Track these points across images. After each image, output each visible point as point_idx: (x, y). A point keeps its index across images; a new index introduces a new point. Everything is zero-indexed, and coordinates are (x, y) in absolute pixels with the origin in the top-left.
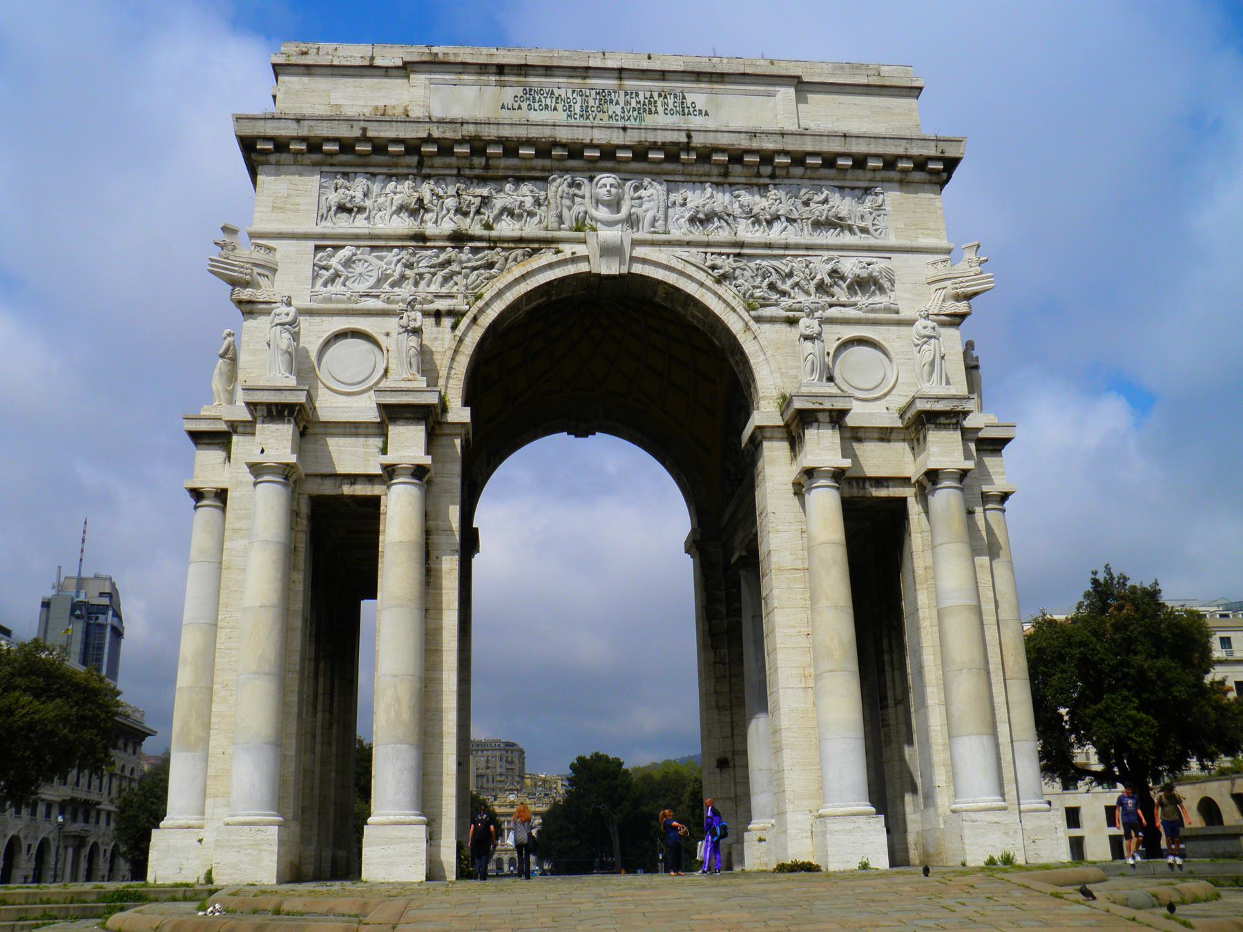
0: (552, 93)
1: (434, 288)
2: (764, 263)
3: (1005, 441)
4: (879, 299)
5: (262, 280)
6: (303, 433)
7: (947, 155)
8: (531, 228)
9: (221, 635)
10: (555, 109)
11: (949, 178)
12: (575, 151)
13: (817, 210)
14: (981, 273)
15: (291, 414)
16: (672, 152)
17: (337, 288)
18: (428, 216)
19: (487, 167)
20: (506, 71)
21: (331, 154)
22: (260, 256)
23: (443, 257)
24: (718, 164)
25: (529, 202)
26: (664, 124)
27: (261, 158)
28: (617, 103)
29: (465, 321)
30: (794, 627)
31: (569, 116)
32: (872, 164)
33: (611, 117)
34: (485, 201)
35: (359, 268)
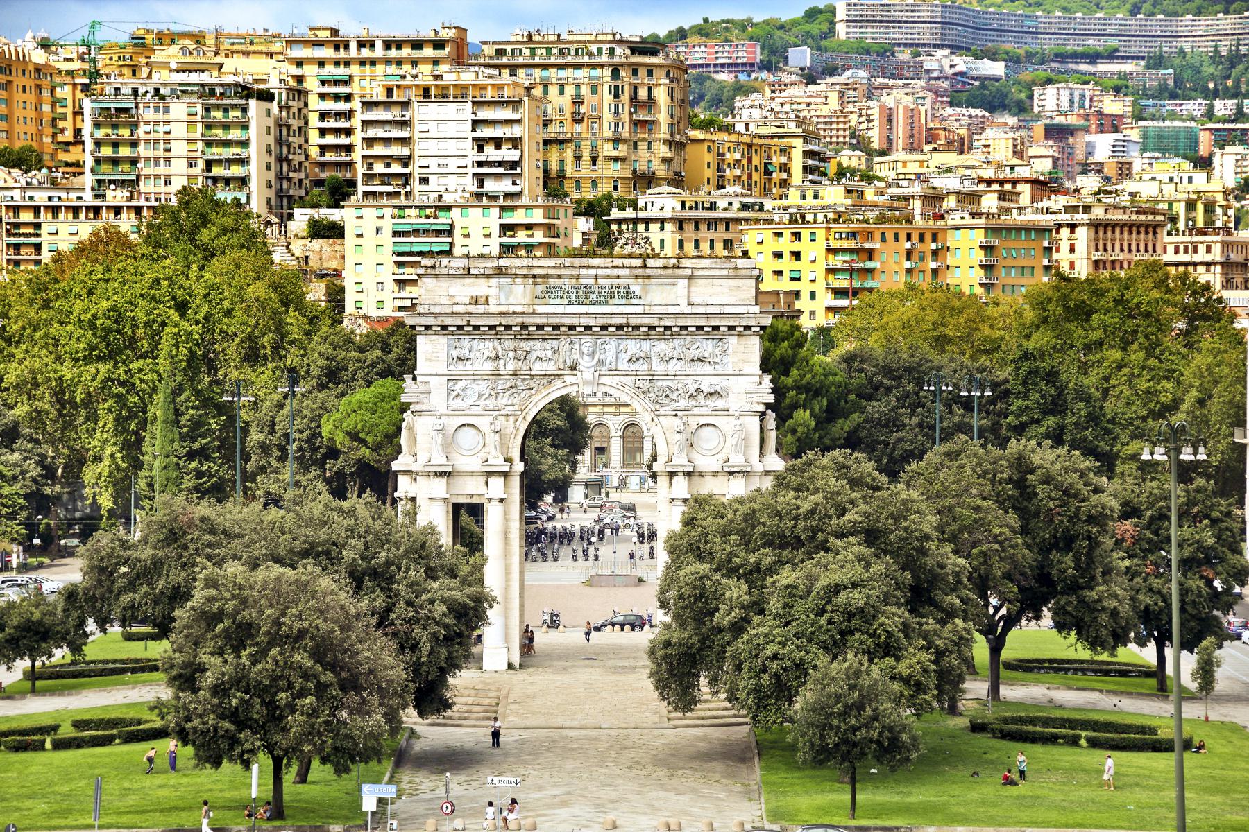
1: (505, 401)
2: (665, 384)
4: (720, 403)
5: (425, 400)
8: (550, 368)
12: (572, 328)
13: (693, 354)
16: (620, 327)
17: (459, 400)
18: (502, 362)
22: (422, 388)
23: (509, 385)
25: (550, 354)
26: (616, 308)
29: (521, 418)
34: (528, 353)
35: (469, 392)
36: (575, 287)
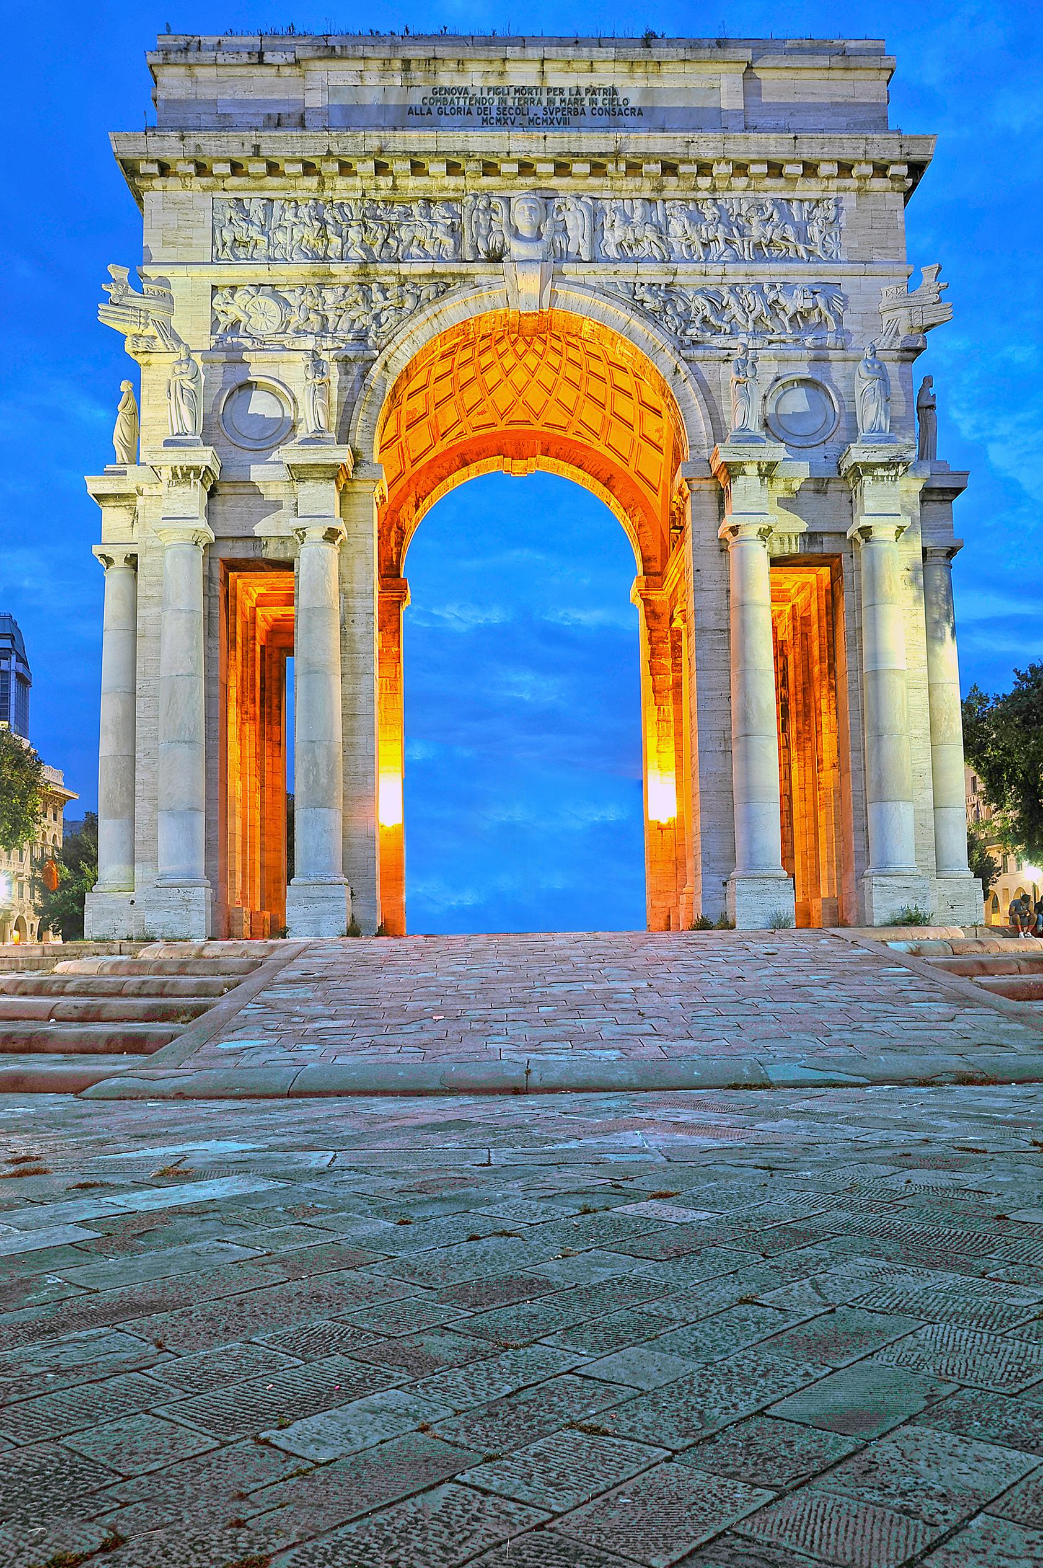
0: (466, 92)
3: (957, 491)
6: (211, 495)
7: (912, 158)
9: (140, 703)
10: (469, 112)
11: (915, 185)
14: (940, 301)
15: (197, 476)
19: (395, 188)
20: (413, 65)
21: (223, 177)
24: (649, 176)
27: (145, 184)
28: (540, 101)
30: (716, 690)
31: (484, 120)
32: (825, 169)
33: (531, 120)
36: (496, 90)
